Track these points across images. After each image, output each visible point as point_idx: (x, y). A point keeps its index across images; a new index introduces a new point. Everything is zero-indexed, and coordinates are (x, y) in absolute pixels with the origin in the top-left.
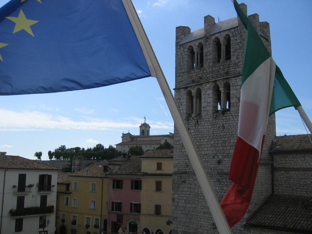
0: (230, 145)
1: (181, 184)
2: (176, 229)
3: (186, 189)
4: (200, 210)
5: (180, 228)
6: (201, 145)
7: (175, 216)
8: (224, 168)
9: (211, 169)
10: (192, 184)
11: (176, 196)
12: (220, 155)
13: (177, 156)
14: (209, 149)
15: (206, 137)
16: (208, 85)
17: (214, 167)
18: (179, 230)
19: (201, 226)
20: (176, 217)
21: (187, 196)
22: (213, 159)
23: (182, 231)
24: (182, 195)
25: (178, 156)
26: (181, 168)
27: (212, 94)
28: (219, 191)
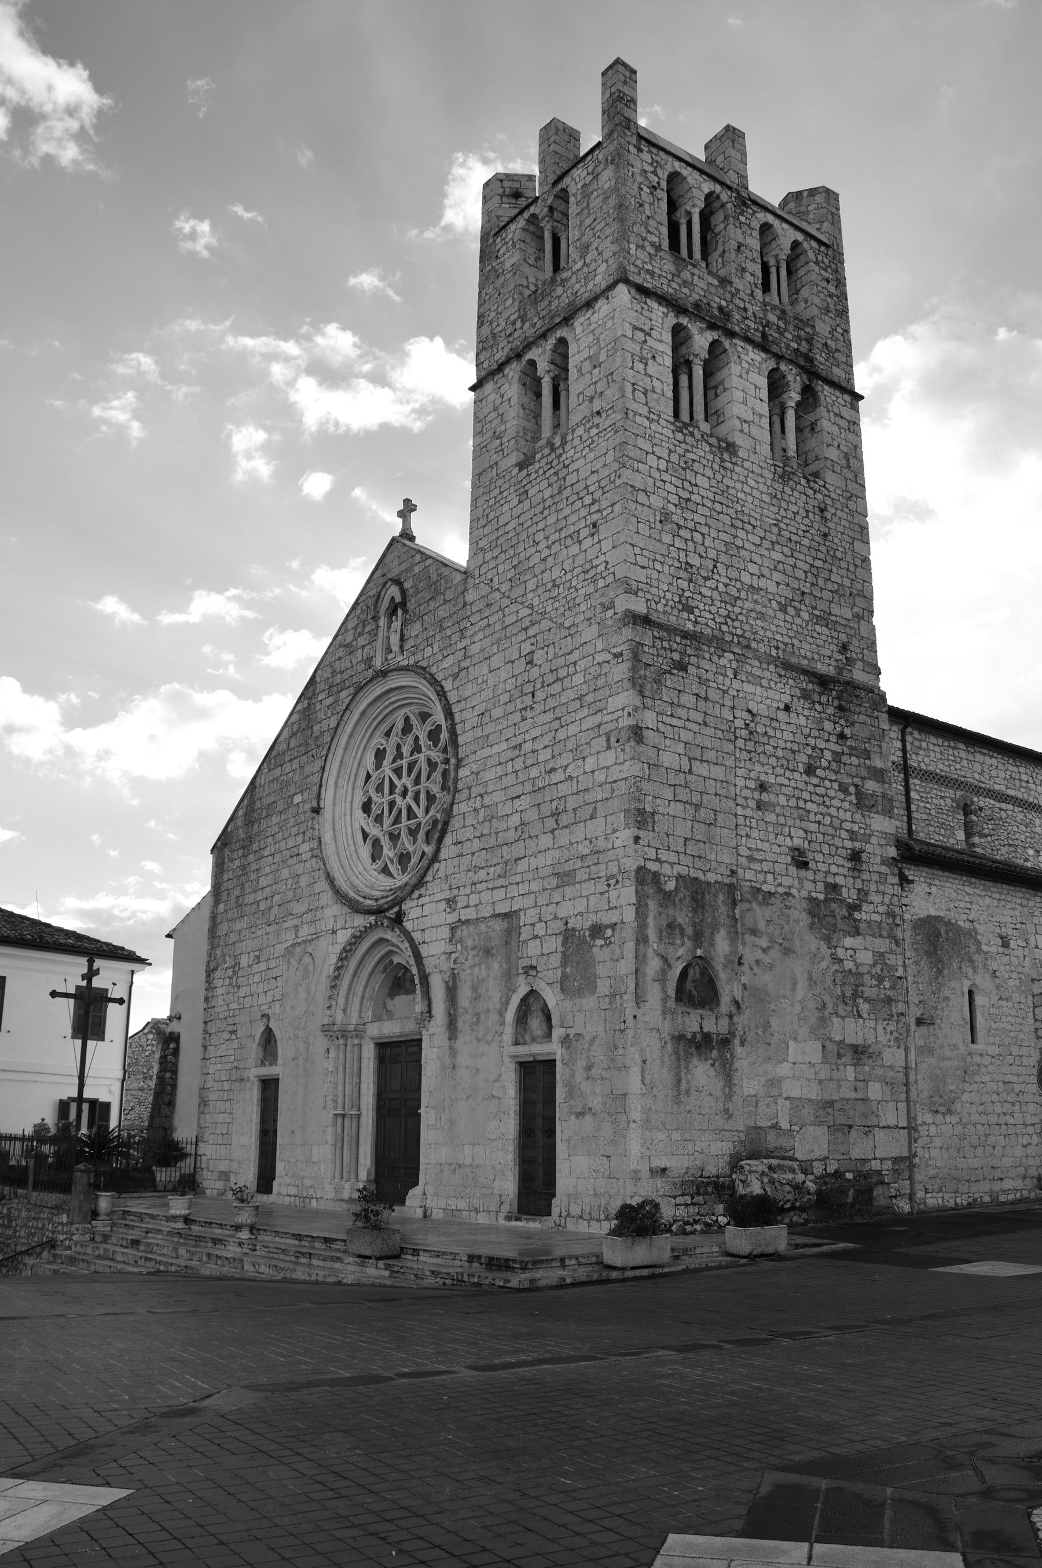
0: (830, 586)
2: (653, 866)
3: (688, 700)
4: (746, 793)
5: (672, 864)
6: (738, 548)
7: (648, 809)
8: (816, 657)
9: (777, 648)
10: (711, 684)
11: (649, 719)
12: (803, 608)
13: (642, 549)
14: (766, 572)
15: (754, 527)
16: (752, 355)
17: (786, 644)
18: (666, 869)
19: (751, 859)
20: (653, 814)
21: (695, 727)
22: (780, 614)
23: (680, 877)
25: (645, 552)
28: (808, 730)
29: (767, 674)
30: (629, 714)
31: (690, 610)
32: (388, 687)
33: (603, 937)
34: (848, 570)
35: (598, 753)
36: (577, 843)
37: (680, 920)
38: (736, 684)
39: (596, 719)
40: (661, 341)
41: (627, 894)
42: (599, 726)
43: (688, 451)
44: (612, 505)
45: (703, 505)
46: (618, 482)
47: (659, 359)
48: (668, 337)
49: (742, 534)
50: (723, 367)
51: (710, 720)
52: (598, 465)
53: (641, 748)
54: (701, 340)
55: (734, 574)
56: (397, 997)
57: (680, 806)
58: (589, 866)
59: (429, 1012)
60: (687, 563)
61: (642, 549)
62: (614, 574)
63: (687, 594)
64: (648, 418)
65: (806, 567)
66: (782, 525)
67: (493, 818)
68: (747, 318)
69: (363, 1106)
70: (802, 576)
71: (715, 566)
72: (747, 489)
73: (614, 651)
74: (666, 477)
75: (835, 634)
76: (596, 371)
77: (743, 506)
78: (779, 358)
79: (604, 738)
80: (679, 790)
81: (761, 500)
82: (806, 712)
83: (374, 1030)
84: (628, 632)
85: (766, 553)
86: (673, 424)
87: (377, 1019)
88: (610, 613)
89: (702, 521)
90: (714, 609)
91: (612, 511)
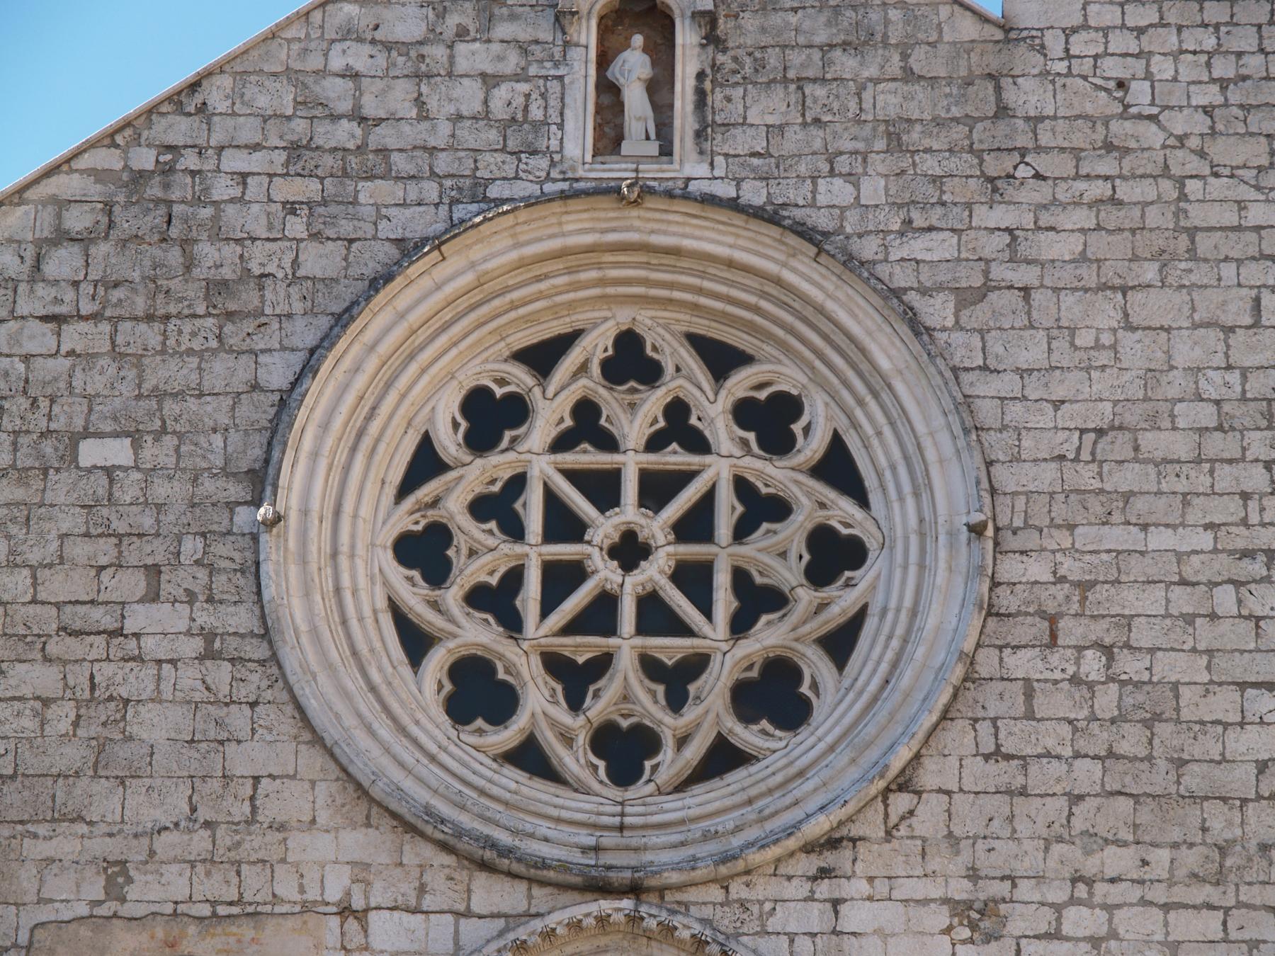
32: (633, 237)
67: (1157, 717)
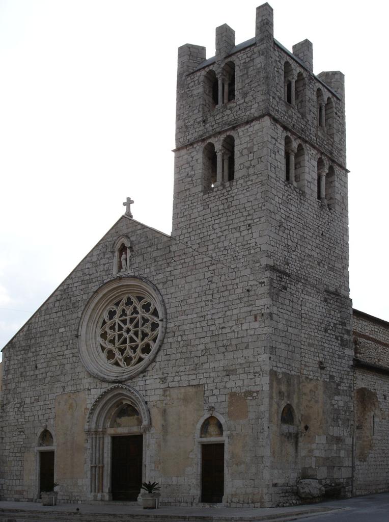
1: (281, 291)
2: (275, 369)
3: (287, 302)
5: (281, 368)
6: (305, 238)
9: (316, 281)
12: (326, 264)
13: (273, 238)
14: (314, 248)
15: (311, 229)
18: (279, 370)
21: (289, 313)
22: (318, 267)
23: (283, 373)
24: (282, 311)
26: (278, 263)
27: (201, 158)
29: (313, 291)
30: (268, 308)
31: (288, 264)
33: (252, 396)
34: (341, 248)
35: (250, 322)
36: (238, 358)
37: (283, 390)
38: (303, 296)
39: (249, 309)
40: (281, 144)
41: (266, 380)
42: (250, 311)
43: (289, 195)
44: (260, 218)
45: (294, 219)
46: (263, 208)
47: (280, 153)
48: (283, 143)
49: (306, 232)
50: (301, 155)
51: (294, 310)
52: (251, 199)
53: (272, 322)
54: (295, 144)
55: (303, 250)
56: (122, 418)
57: (284, 345)
58: (244, 368)
59: (151, 424)
60: (287, 244)
61: (273, 238)
62: (260, 248)
63: (287, 257)
64: (276, 180)
65: (327, 246)
66: (320, 229)
68: (311, 134)
69: (105, 462)
70: (326, 250)
71: (297, 246)
72: (309, 212)
73: (260, 281)
74: (281, 206)
75: (335, 275)
76: (252, 155)
77: (307, 220)
78: (322, 153)
79: (253, 317)
80: (284, 339)
81: (313, 217)
82: (325, 307)
83: (111, 431)
84: (268, 274)
85: (314, 240)
86: (284, 182)
87: (112, 426)
88: (258, 265)
89: (293, 226)
90: (296, 264)
91: (260, 221)
